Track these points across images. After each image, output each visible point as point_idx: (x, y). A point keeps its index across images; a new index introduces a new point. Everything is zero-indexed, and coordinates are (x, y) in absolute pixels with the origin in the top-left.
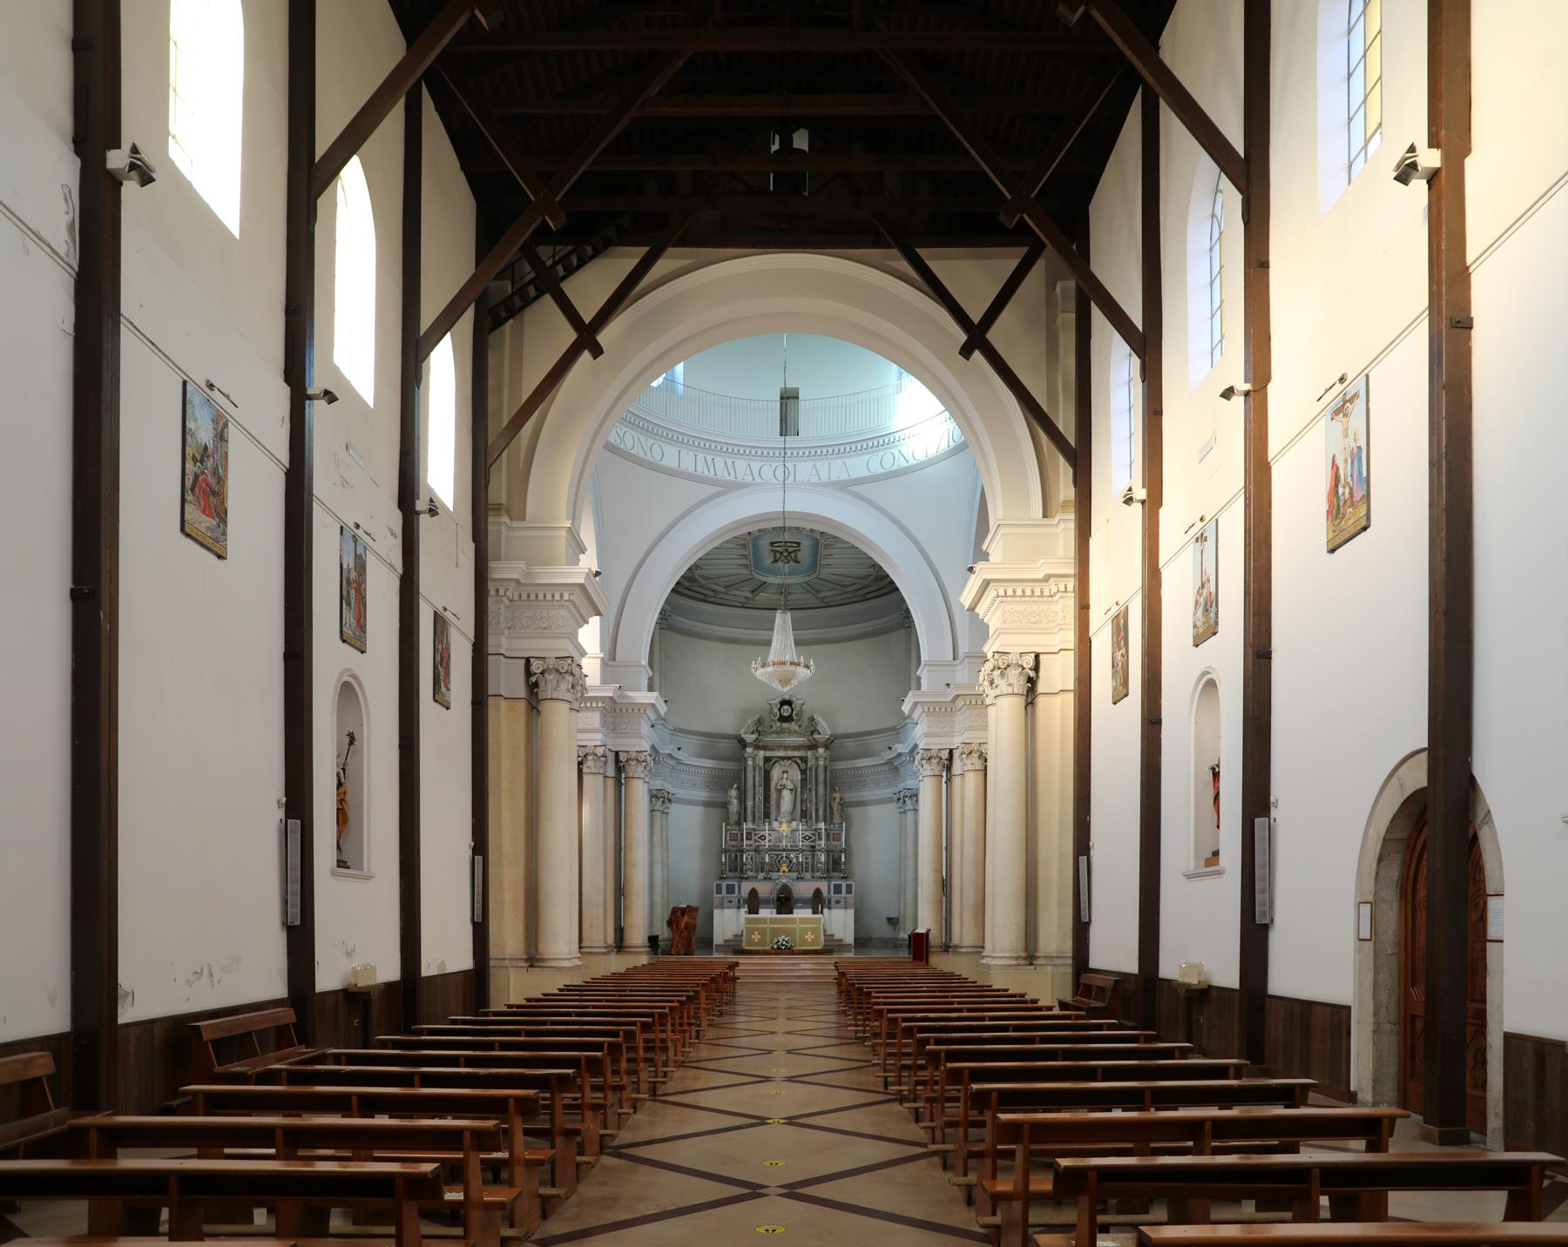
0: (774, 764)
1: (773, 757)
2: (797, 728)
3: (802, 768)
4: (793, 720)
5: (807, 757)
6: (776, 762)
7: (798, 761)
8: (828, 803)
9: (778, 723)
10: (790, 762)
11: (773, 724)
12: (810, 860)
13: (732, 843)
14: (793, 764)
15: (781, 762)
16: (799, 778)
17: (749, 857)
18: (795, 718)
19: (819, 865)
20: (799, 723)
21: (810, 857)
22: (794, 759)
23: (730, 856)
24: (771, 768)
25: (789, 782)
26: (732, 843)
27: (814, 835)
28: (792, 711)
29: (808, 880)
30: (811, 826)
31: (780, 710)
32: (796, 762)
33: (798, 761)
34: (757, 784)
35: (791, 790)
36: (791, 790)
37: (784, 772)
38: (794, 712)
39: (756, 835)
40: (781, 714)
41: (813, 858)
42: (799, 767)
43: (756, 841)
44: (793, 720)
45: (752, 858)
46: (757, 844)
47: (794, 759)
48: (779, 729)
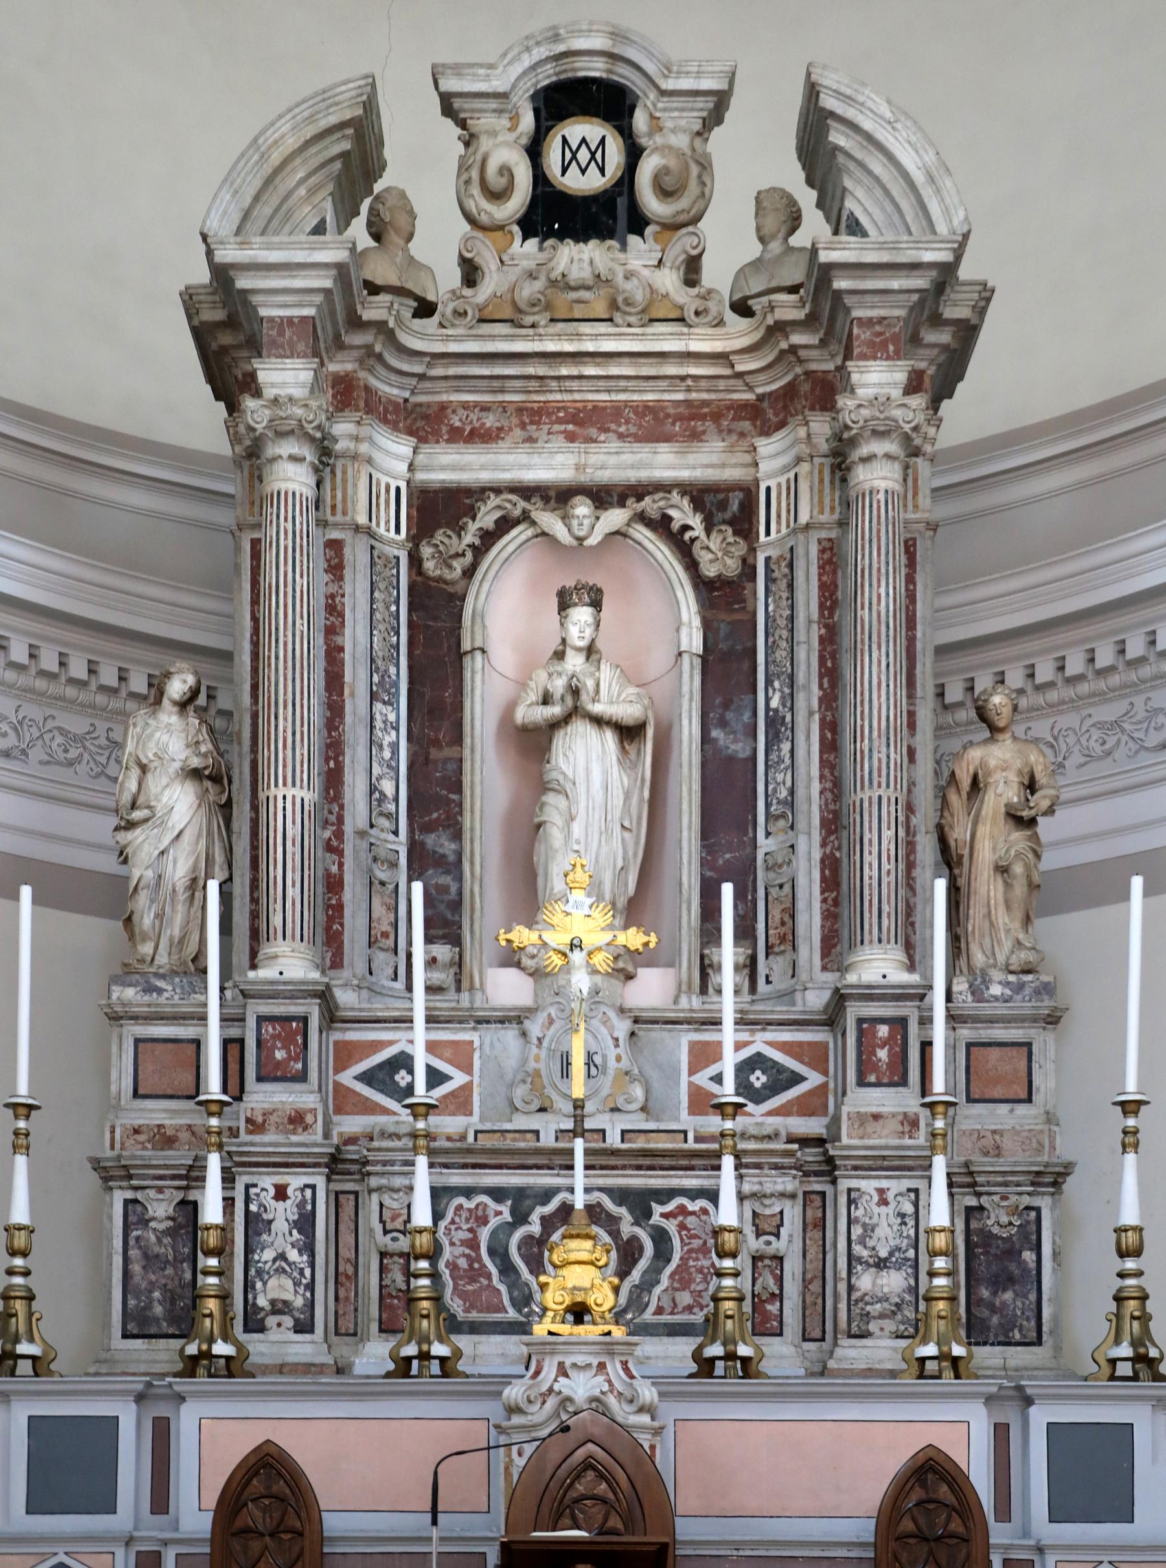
0: (489, 538)
1: (482, 492)
2: (669, 281)
3: (710, 570)
4: (638, 223)
5: (749, 493)
6: (505, 524)
7: (683, 514)
8: (924, 820)
9: (527, 250)
10: (615, 517)
11: (488, 260)
12: (789, 1242)
13: (156, 1113)
14: (642, 533)
15: (549, 521)
16: (693, 639)
17: (282, 1214)
18: (651, 203)
19: (865, 1281)
20: (683, 243)
21: (793, 1214)
22: (651, 505)
23: (135, 1215)
24: (469, 573)
25: (606, 673)
26: (156, 1113)
27: (816, 1057)
28: (634, 153)
29: (784, 1394)
30: (787, 996)
31: (535, 151)
32: (661, 525)
33: (683, 514)
34: (356, 677)
35: (629, 733)
36: (629, 733)
37: (564, 602)
38: (647, 168)
39: (346, 1055)
40: (540, 178)
41: (816, 1225)
42: (692, 566)
43: (344, 1101)
44: (638, 223)
45: (305, 1223)
46: (351, 1124)
47: (651, 505)
48: (529, 291)
